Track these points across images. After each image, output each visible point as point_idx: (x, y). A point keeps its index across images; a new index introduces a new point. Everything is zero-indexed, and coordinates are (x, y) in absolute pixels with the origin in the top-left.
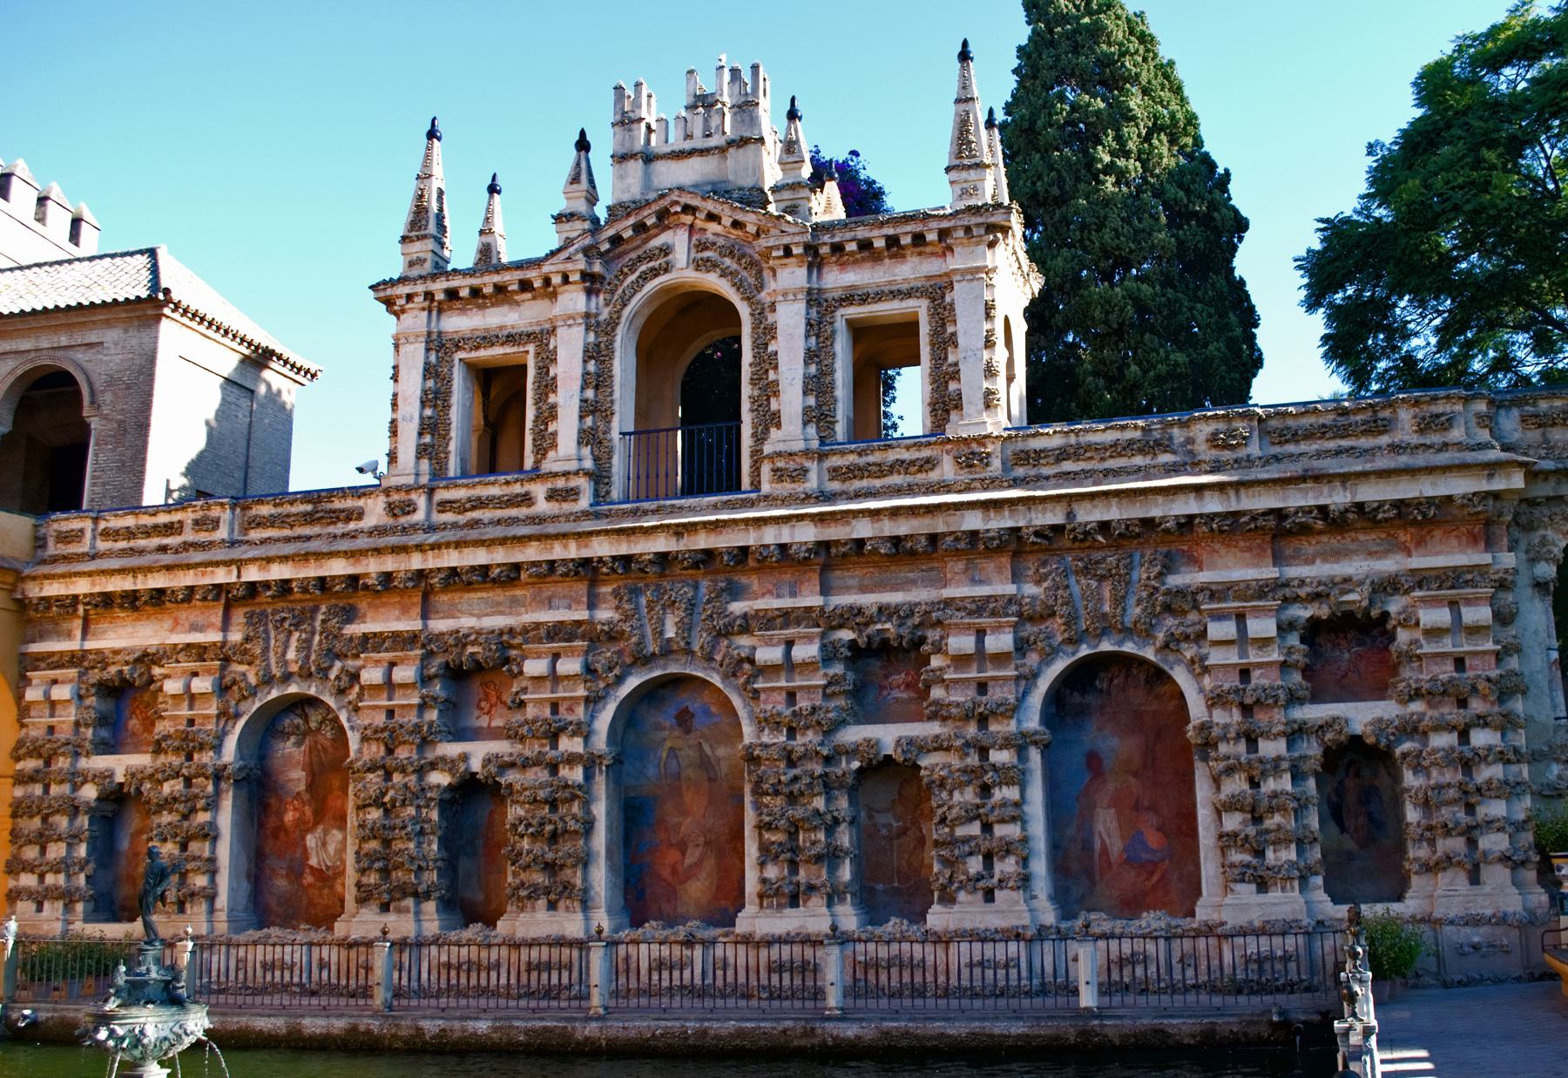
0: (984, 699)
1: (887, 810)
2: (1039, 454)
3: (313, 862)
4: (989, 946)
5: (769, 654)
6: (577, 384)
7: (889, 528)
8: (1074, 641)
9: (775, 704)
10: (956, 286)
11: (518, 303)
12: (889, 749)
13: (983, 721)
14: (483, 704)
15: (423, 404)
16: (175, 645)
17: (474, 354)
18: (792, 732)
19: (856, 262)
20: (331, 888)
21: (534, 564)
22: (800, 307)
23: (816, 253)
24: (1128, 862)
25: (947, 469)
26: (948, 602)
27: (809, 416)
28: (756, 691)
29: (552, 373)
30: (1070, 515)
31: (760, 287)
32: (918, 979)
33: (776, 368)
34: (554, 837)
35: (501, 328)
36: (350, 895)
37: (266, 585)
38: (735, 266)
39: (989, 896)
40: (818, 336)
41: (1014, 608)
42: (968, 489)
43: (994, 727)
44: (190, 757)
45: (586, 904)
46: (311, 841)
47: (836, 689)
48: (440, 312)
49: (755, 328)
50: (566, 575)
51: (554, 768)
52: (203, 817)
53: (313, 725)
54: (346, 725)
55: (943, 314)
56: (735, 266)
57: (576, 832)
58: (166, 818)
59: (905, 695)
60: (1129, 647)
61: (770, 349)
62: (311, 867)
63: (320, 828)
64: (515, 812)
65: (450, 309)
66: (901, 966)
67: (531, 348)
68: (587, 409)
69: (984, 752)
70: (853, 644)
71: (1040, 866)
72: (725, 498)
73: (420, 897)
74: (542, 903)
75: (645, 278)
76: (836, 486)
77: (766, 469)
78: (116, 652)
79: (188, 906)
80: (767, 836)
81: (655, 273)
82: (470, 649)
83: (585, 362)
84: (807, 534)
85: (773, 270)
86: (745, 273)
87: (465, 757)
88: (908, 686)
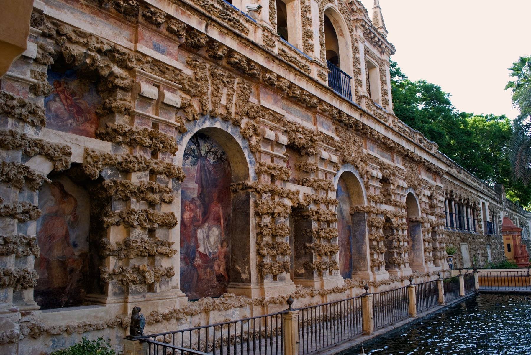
3: (201, 249)
16: (144, 55)
20: (212, 267)
28: (370, 185)
44: (154, 155)
46: (200, 234)
49: (353, 45)
62: (200, 253)
63: (206, 225)
64: (315, 226)
79: (157, 285)
82: (300, 136)
87: (298, 192)
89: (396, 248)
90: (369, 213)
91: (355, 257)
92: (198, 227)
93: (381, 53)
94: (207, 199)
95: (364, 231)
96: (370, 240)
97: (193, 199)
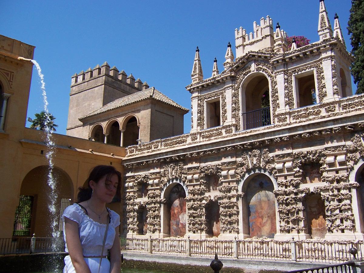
0: (337, 175)
1: (315, 207)
3: (181, 222)
4: (344, 246)
6: (231, 103)
9: (282, 180)
10: (323, 62)
11: (217, 86)
12: (312, 190)
13: (338, 181)
14: (215, 183)
15: (198, 113)
17: (208, 100)
18: (286, 187)
19: (296, 61)
21: (223, 148)
23: (285, 61)
25: (323, 113)
27: (287, 104)
28: (277, 176)
29: (225, 102)
31: (272, 73)
32: (323, 255)
33: (277, 92)
34: (230, 216)
35: (214, 92)
36: (187, 229)
37: (167, 158)
38: (266, 68)
39: (343, 231)
40: (287, 82)
41: (346, 148)
42: (329, 116)
44: (155, 198)
45: (238, 233)
46: (180, 217)
47: (297, 174)
48: (201, 91)
50: (230, 149)
52: (157, 212)
53: (180, 190)
54: (185, 189)
55: (320, 71)
57: (235, 214)
58: (151, 212)
61: (276, 87)
63: (182, 214)
66: (318, 251)
67: (221, 96)
68: (234, 110)
69: (339, 190)
70: (301, 163)
72: (266, 127)
73: (202, 230)
74: (228, 231)
76: (295, 121)
78: (141, 176)
81: (248, 73)
82: (210, 170)
83: (232, 98)
89: (328, 216)
92: (180, 214)
94: (182, 205)
97: (177, 206)
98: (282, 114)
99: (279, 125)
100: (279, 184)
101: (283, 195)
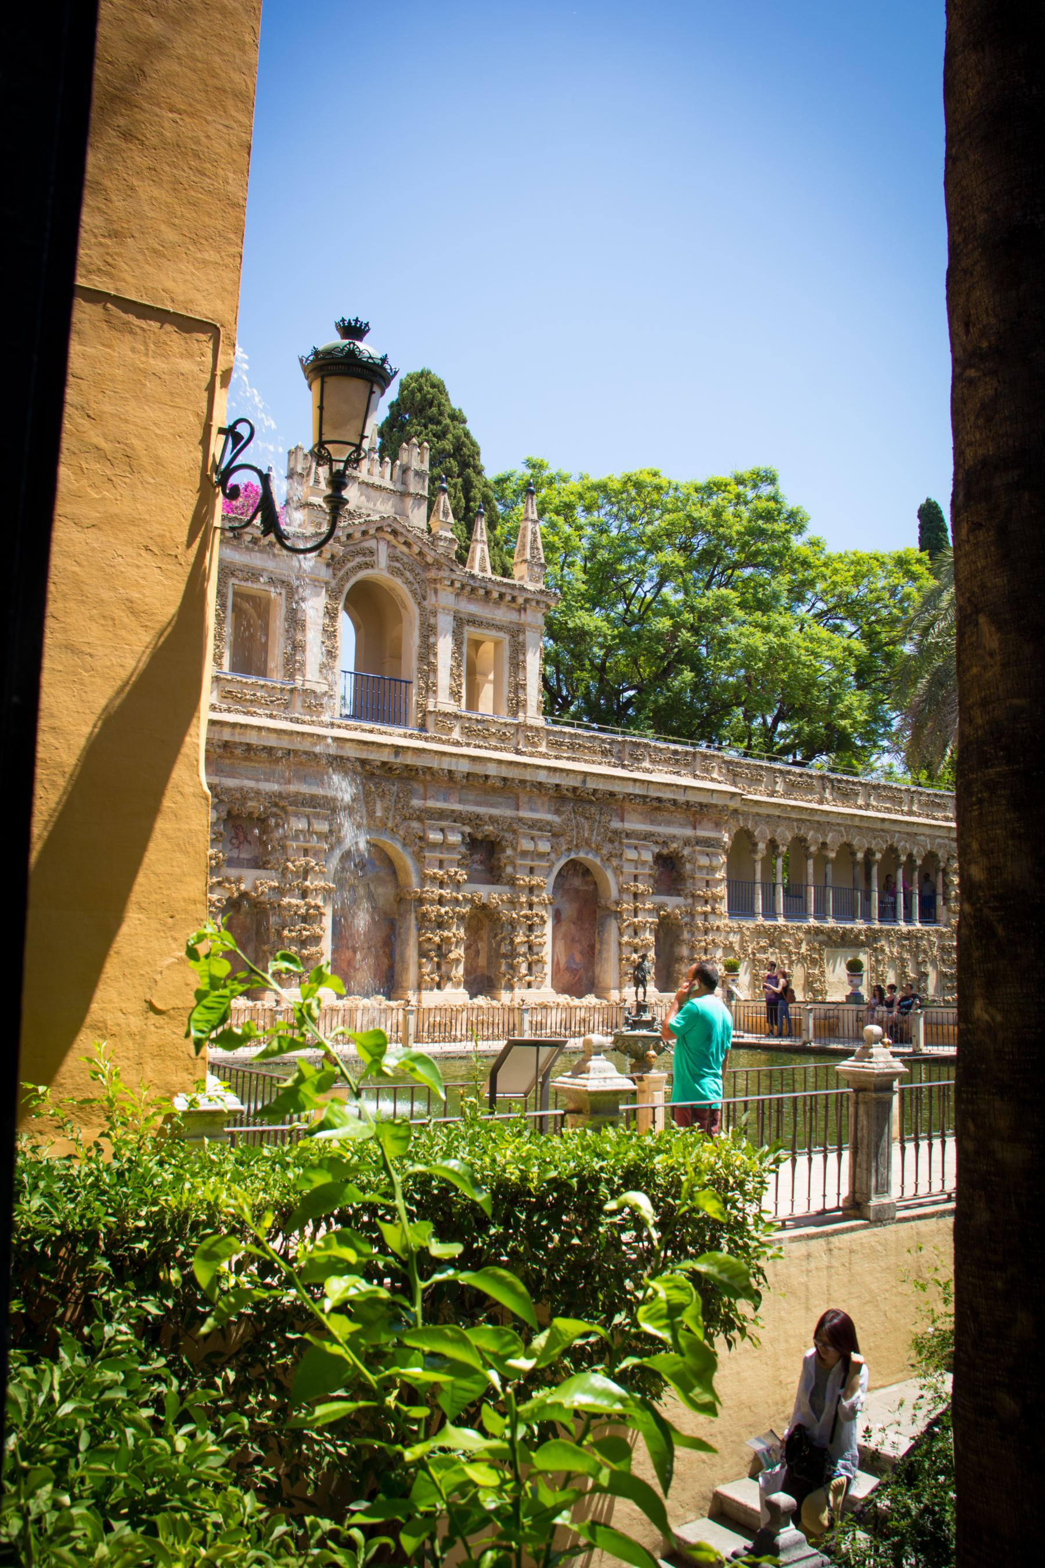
2: (562, 744)
5: (435, 836)
7: (505, 772)
8: (569, 850)
22: (450, 618)
24: (567, 969)
26: (520, 820)
30: (584, 782)
31: (424, 598)
33: (435, 655)
34: (303, 943)
38: (411, 578)
43: (536, 892)
49: (422, 624)
51: (304, 894)
56: (411, 578)
59: (479, 868)
60: (590, 856)
65: (227, 543)
71: (548, 969)
75: (360, 567)
77: (430, 721)
80: (427, 946)
82: (250, 804)
84: (464, 767)
85: (436, 591)
86: (416, 586)
88: (482, 862)
89: (505, 956)
90: (421, 901)
91: (398, 967)
93: (519, 611)
95: (408, 928)
96: (420, 943)
98: (446, 715)
99: (440, 739)
100: (424, 879)
101: (432, 902)
